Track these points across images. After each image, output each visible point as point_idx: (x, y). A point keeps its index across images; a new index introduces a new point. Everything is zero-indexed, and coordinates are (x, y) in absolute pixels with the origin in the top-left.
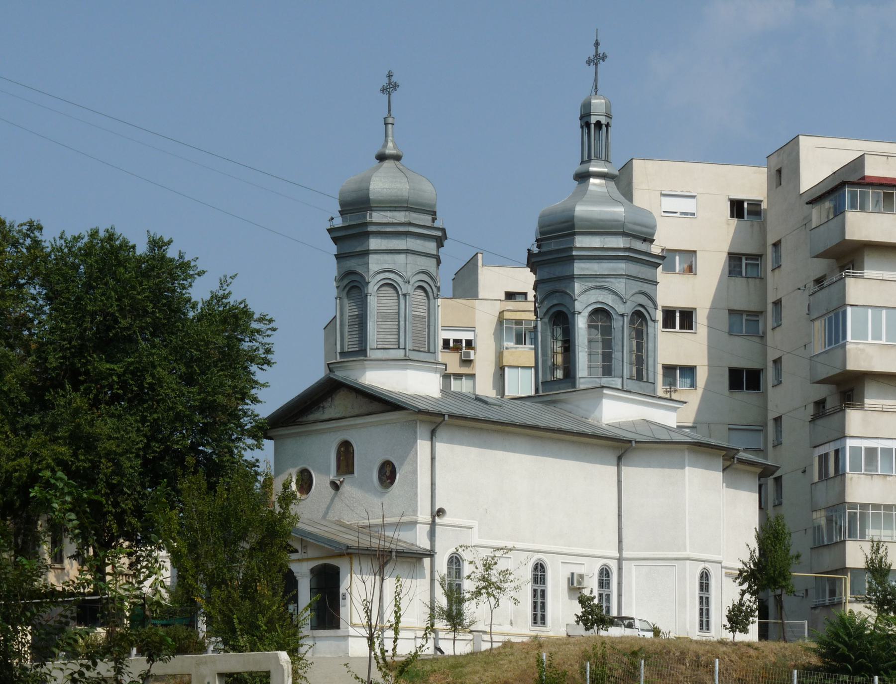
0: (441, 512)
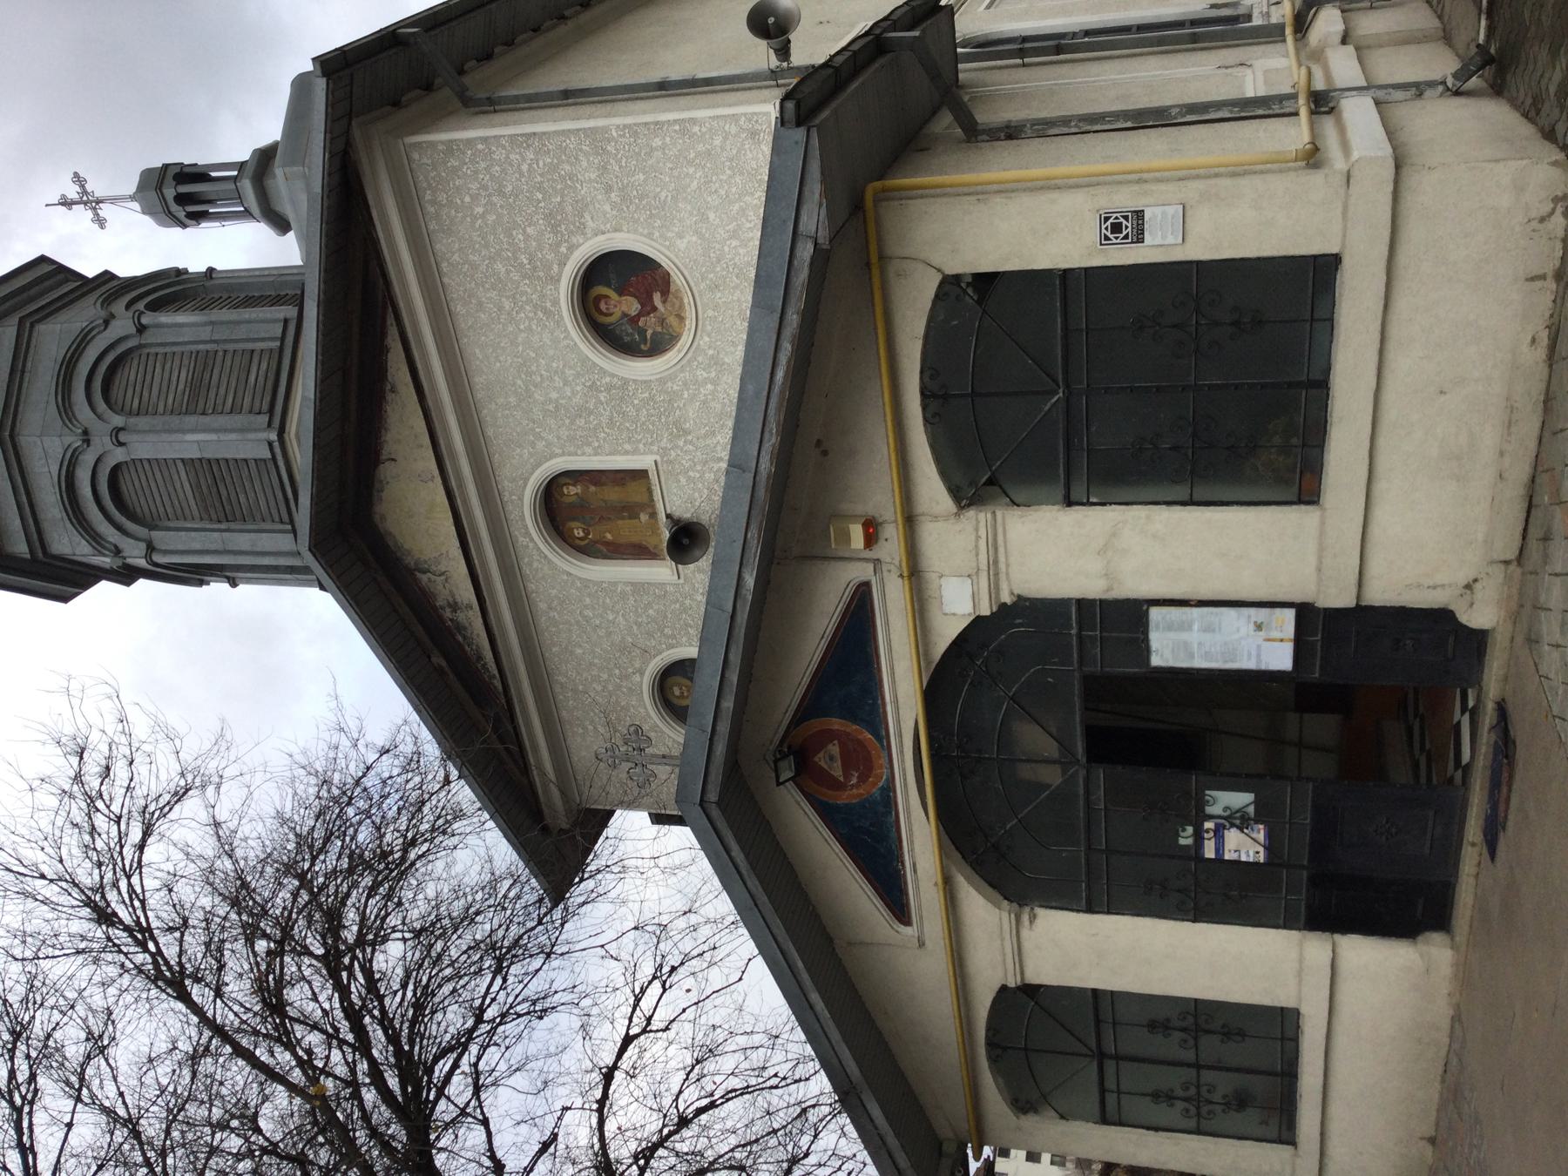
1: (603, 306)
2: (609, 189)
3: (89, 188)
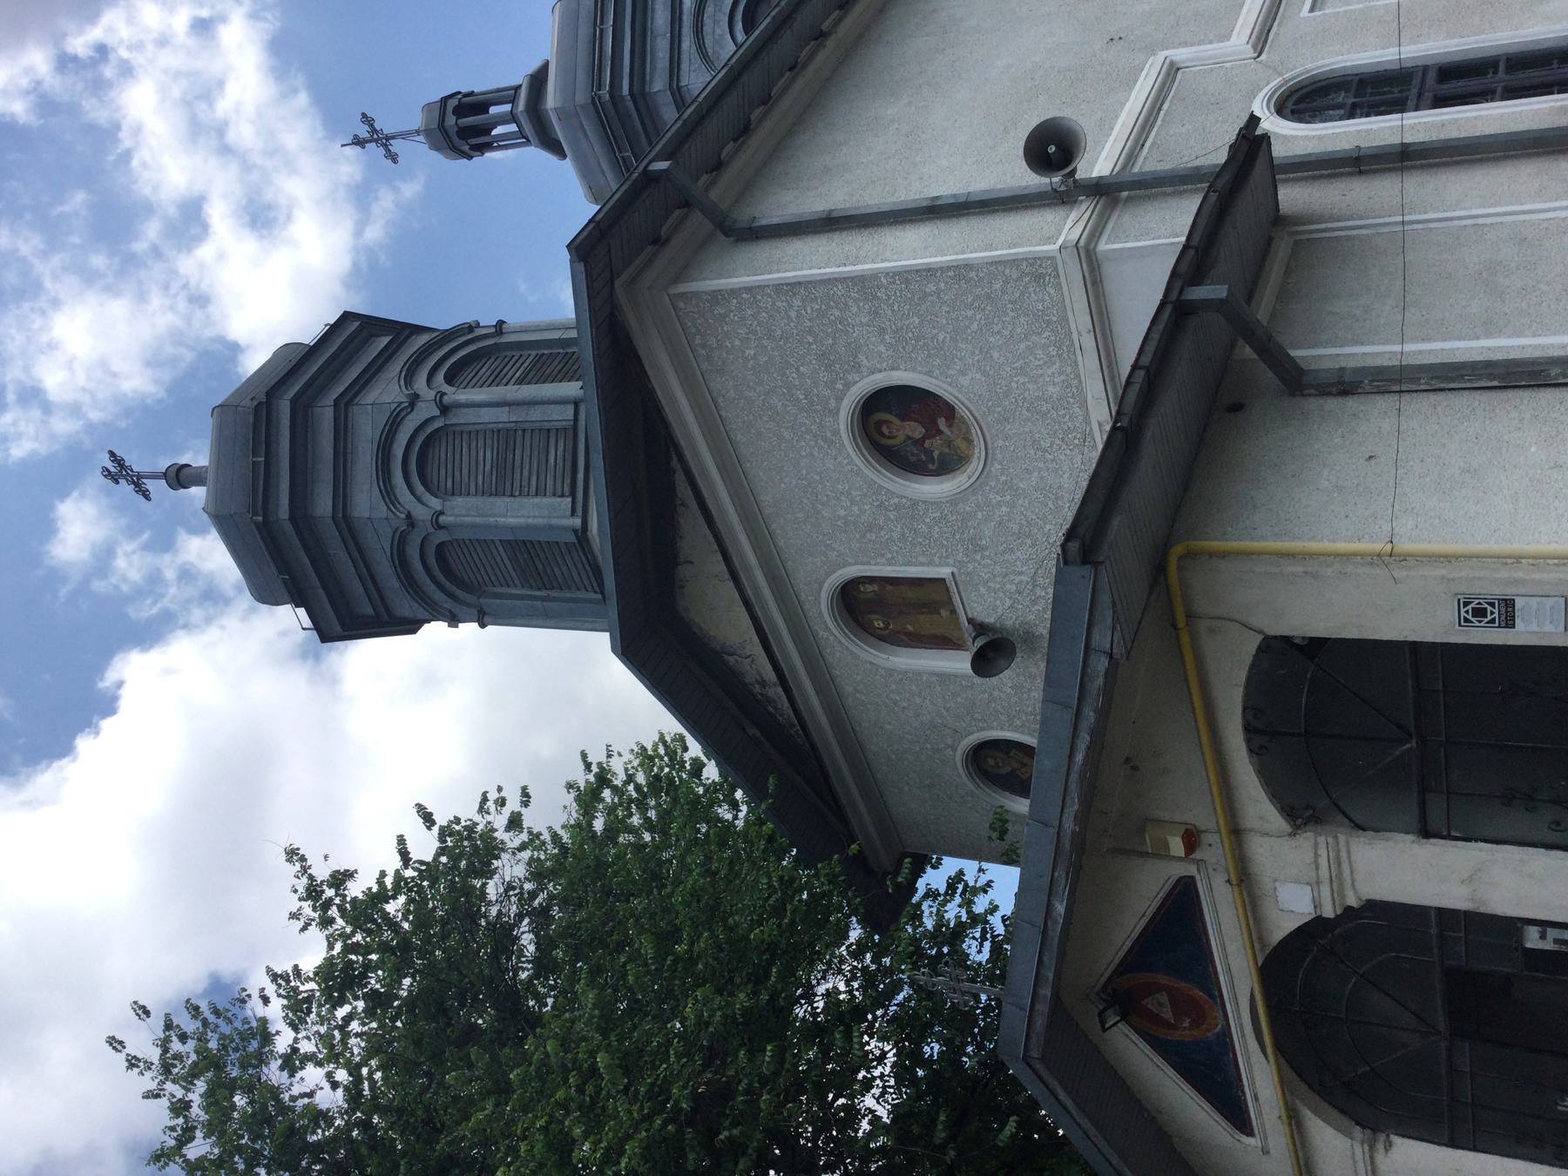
0: (1052, 148)
1: (885, 430)
2: (882, 331)
3: (377, 126)
